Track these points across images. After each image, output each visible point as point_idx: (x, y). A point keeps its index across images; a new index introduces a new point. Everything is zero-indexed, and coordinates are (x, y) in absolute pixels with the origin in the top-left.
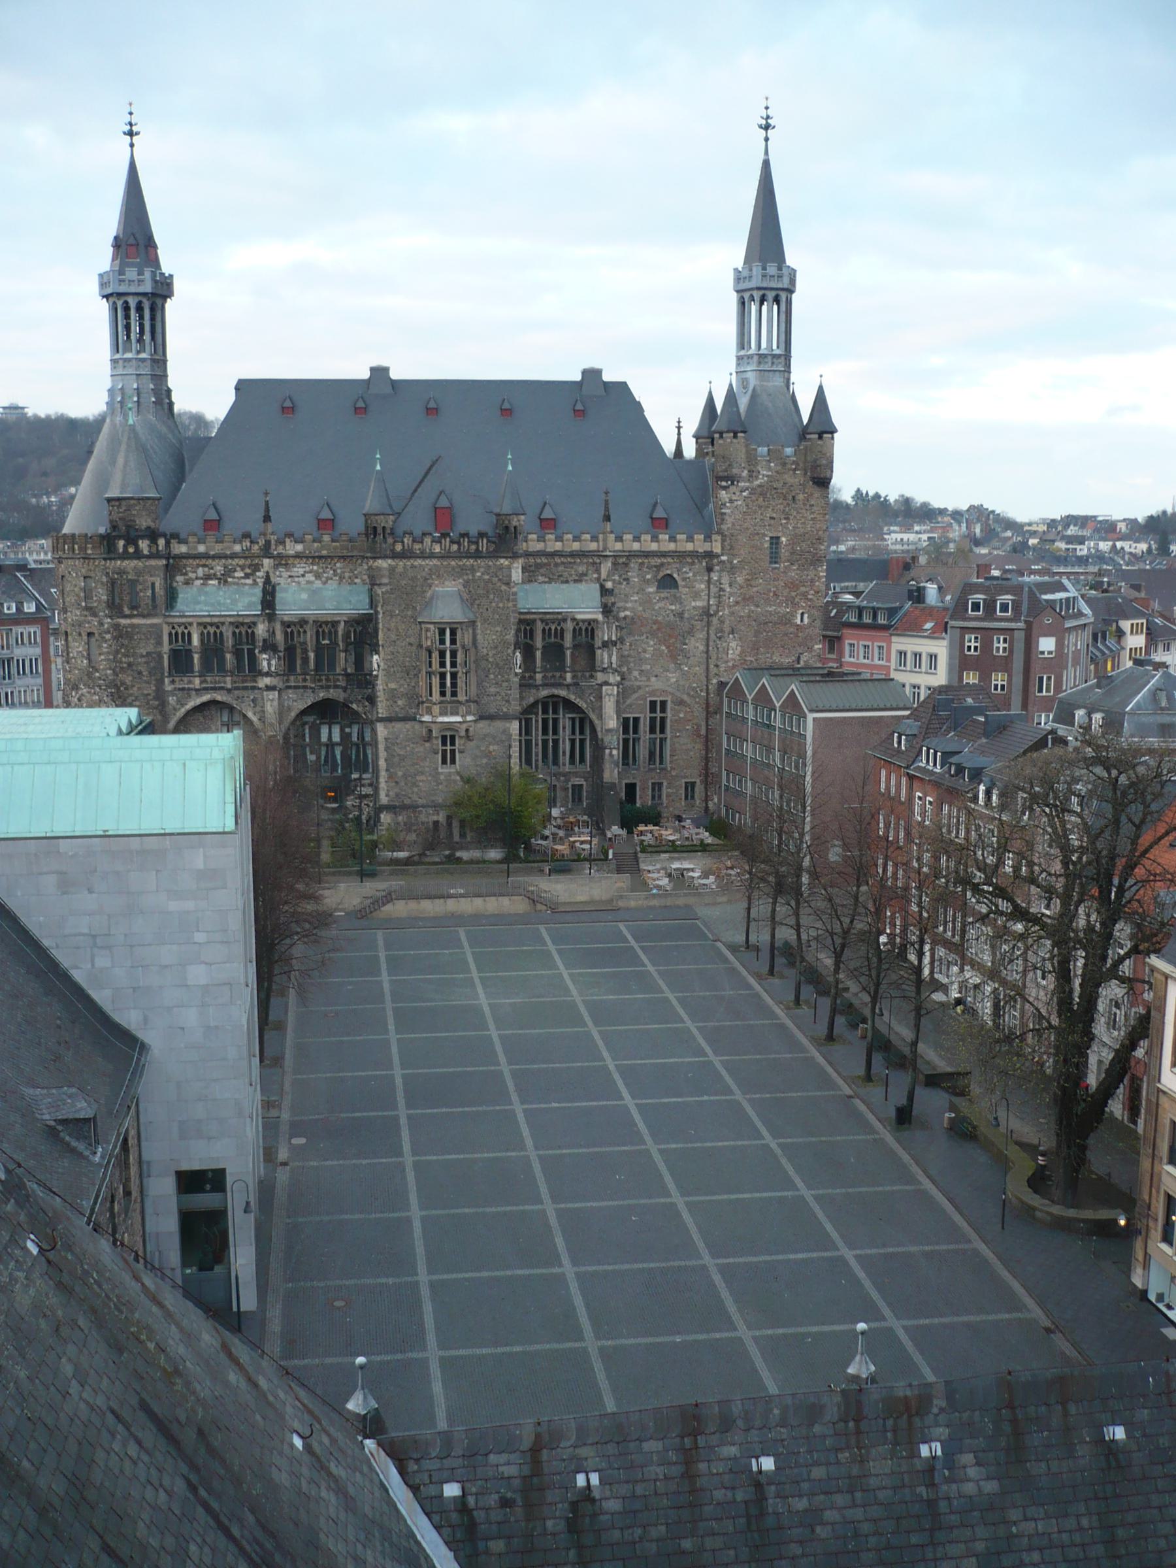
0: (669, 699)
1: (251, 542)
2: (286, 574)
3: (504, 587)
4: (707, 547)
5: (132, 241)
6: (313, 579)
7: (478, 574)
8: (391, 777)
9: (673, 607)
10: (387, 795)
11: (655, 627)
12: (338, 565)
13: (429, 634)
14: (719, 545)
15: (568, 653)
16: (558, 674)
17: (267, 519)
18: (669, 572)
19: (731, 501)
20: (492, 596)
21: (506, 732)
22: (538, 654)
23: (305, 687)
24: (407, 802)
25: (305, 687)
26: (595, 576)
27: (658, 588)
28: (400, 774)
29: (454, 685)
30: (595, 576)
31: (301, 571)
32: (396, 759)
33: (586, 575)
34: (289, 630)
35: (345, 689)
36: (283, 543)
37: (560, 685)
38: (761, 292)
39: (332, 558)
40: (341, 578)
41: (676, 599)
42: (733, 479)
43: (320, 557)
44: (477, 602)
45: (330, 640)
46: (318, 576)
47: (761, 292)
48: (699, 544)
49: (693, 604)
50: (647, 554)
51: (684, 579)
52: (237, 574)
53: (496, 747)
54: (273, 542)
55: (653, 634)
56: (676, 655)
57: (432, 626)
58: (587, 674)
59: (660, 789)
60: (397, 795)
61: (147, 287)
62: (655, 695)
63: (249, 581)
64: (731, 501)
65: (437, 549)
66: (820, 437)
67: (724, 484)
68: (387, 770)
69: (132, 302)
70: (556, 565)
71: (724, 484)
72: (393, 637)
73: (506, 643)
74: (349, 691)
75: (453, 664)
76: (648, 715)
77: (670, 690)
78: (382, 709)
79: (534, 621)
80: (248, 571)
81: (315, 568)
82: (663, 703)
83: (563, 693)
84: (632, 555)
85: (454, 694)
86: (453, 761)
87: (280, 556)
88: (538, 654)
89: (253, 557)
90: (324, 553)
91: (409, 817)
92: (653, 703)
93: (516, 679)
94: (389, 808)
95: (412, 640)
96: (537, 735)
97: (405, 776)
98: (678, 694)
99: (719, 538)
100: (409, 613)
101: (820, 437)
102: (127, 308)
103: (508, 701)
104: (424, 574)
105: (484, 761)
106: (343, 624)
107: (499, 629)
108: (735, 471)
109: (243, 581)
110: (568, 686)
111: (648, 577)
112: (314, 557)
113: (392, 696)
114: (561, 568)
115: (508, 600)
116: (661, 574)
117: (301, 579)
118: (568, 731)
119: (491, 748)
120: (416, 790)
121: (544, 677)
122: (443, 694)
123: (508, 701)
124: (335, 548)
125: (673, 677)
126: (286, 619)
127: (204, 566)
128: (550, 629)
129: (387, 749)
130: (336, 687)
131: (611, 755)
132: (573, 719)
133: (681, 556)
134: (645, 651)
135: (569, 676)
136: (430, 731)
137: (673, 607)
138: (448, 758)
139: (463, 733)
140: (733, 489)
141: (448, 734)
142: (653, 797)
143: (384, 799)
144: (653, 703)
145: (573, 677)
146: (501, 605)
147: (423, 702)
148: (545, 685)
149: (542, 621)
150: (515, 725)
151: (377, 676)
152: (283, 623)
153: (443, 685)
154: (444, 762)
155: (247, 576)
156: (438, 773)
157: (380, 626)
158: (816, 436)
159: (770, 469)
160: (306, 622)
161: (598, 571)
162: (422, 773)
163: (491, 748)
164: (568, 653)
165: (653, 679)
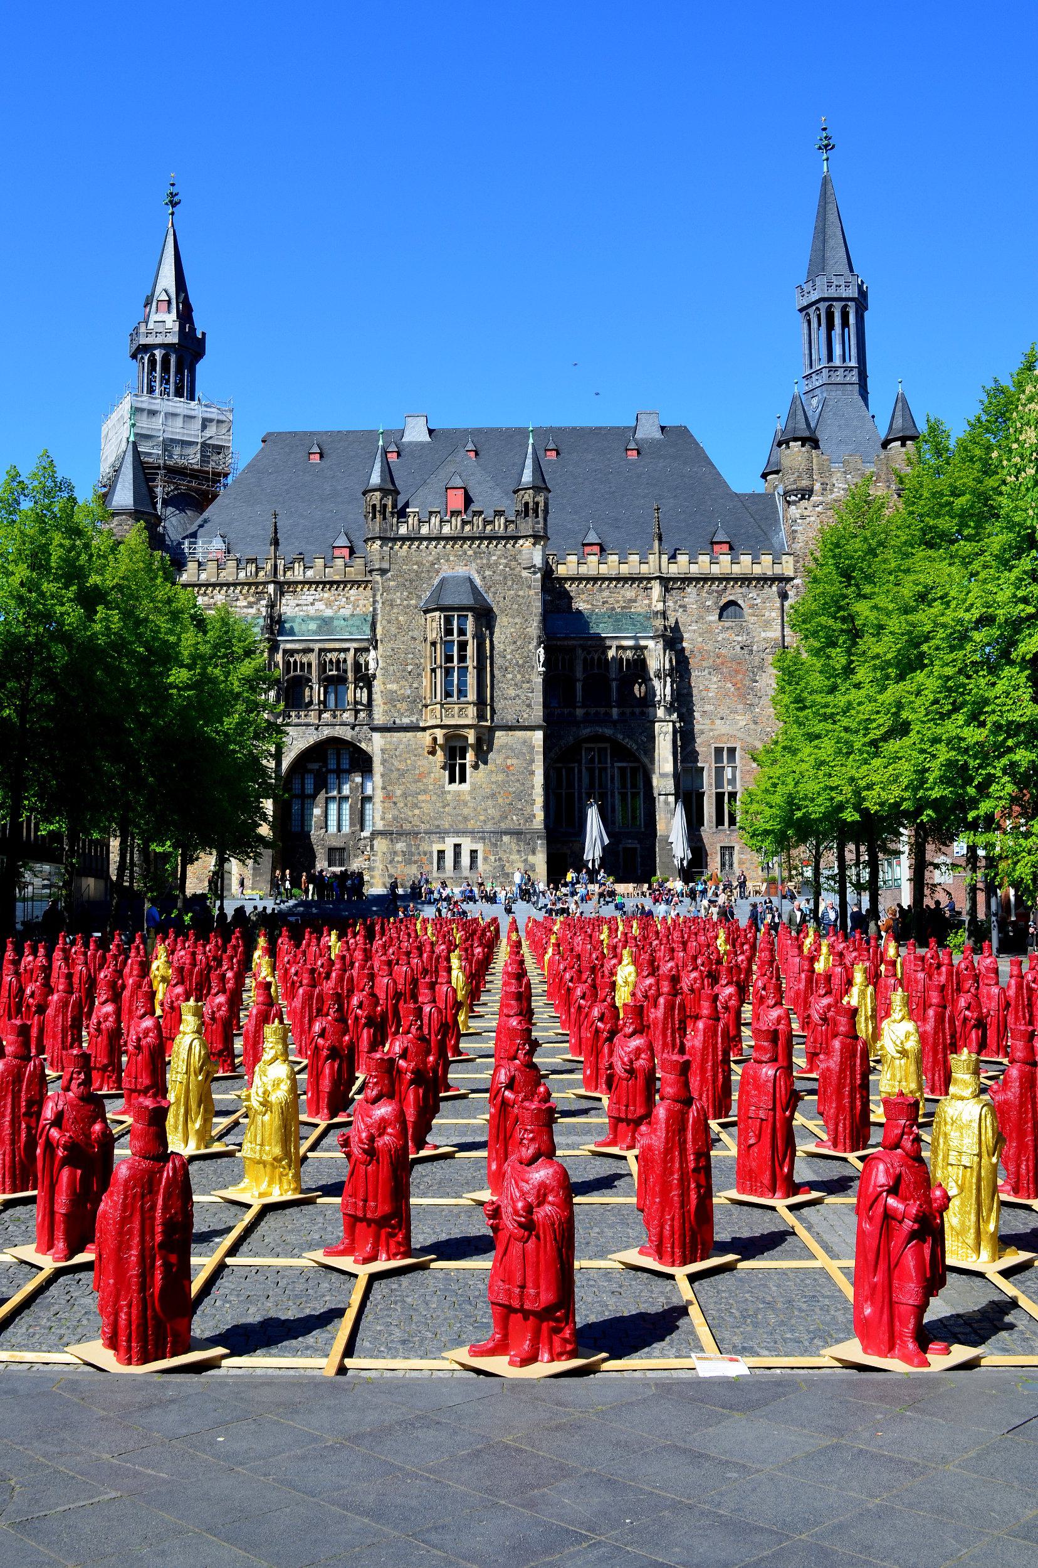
0: (738, 745)
1: (257, 568)
2: (293, 603)
3: (525, 574)
4: (778, 570)
5: (164, 297)
6: (324, 607)
7: (494, 558)
8: (388, 797)
9: (740, 638)
10: (383, 819)
11: (718, 661)
12: (352, 592)
13: (434, 624)
14: (791, 565)
15: (614, 684)
16: (602, 710)
17: (276, 542)
18: (732, 598)
19: (803, 517)
20: (510, 583)
21: (527, 743)
22: (579, 685)
23: (307, 725)
24: (407, 827)
25: (307, 725)
26: (646, 602)
27: (721, 616)
28: (399, 793)
29: (462, 683)
30: (646, 602)
31: (310, 599)
32: (395, 775)
33: (635, 601)
34: (292, 660)
35: (353, 728)
36: (293, 568)
37: (606, 720)
38: (827, 304)
39: (345, 583)
40: (355, 606)
41: (742, 629)
42: (806, 494)
43: (332, 583)
44: (492, 589)
45: (338, 669)
46: (329, 604)
47: (827, 304)
48: (765, 566)
49: (763, 635)
50: (705, 579)
51: (752, 606)
52: (238, 604)
53: (514, 761)
54: (281, 568)
55: (716, 669)
56: (746, 695)
57: (437, 614)
58: (637, 710)
59: (731, 855)
60: (395, 818)
61: (174, 339)
62: (721, 742)
63: (253, 611)
64: (803, 517)
65: (446, 530)
66: (903, 445)
67: (793, 498)
68: (384, 788)
69: (158, 354)
70: (601, 590)
71: (793, 498)
72: (393, 630)
73: (527, 639)
74: (357, 728)
75: (462, 659)
76: (713, 765)
77: (739, 735)
78: (379, 718)
79: (573, 649)
80: (252, 599)
81: (326, 595)
82: (732, 751)
83: (608, 732)
84: (687, 580)
85: (462, 693)
86: (463, 780)
87: (289, 583)
88: (579, 685)
89: (257, 584)
90: (337, 578)
91: (409, 845)
92: (719, 751)
93: (540, 680)
94: (382, 833)
95: (416, 634)
96: (580, 786)
97: (405, 795)
98: (749, 739)
99: (791, 559)
100: (413, 602)
101: (903, 445)
102: (152, 362)
103: (529, 706)
104: (431, 558)
105: (501, 777)
106: (352, 652)
107: (517, 620)
108: (805, 483)
109: (245, 610)
110: (615, 723)
111: (708, 603)
112: (324, 583)
113: (392, 699)
114: (606, 593)
115: (529, 587)
116: (724, 601)
117: (310, 607)
118: (617, 783)
119: (509, 762)
120: (417, 812)
121: (587, 714)
122: (448, 694)
123: (529, 706)
124: (350, 573)
125: (742, 720)
126: (289, 646)
127: (205, 594)
128: (592, 659)
129: (384, 762)
130: (343, 724)
131: (667, 803)
132: (622, 770)
133: (745, 580)
134: (707, 689)
135: (615, 711)
136: (435, 739)
137: (740, 638)
138: (457, 774)
139: (471, 740)
140: (804, 503)
141: (459, 744)
142: (723, 865)
143: (380, 826)
144: (719, 751)
145: (622, 714)
146: (521, 593)
147: (426, 706)
148: (588, 720)
149: (584, 648)
150: (539, 735)
151: (374, 676)
152: (285, 651)
153: (448, 683)
154: (452, 780)
155: (250, 605)
156: (444, 793)
157: (379, 617)
158: (899, 443)
159: (846, 482)
160: (312, 650)
161: (649, 597)
162: (425, 792)
163: (509, 762)
164: (614, 684)
165: (718, 722)
